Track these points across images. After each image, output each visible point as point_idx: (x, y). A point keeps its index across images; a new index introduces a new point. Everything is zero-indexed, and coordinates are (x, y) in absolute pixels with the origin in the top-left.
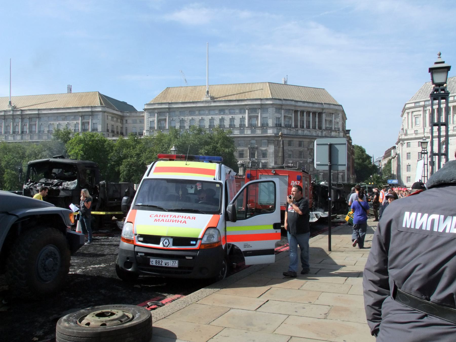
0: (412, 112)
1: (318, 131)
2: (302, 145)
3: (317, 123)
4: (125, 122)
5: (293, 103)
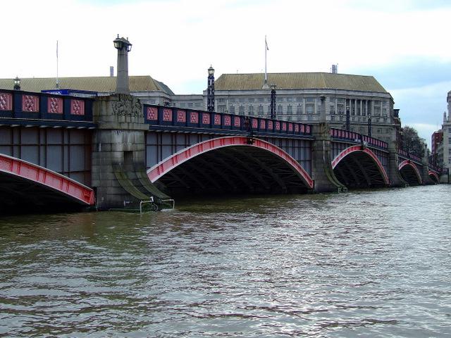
5: (345, 93)
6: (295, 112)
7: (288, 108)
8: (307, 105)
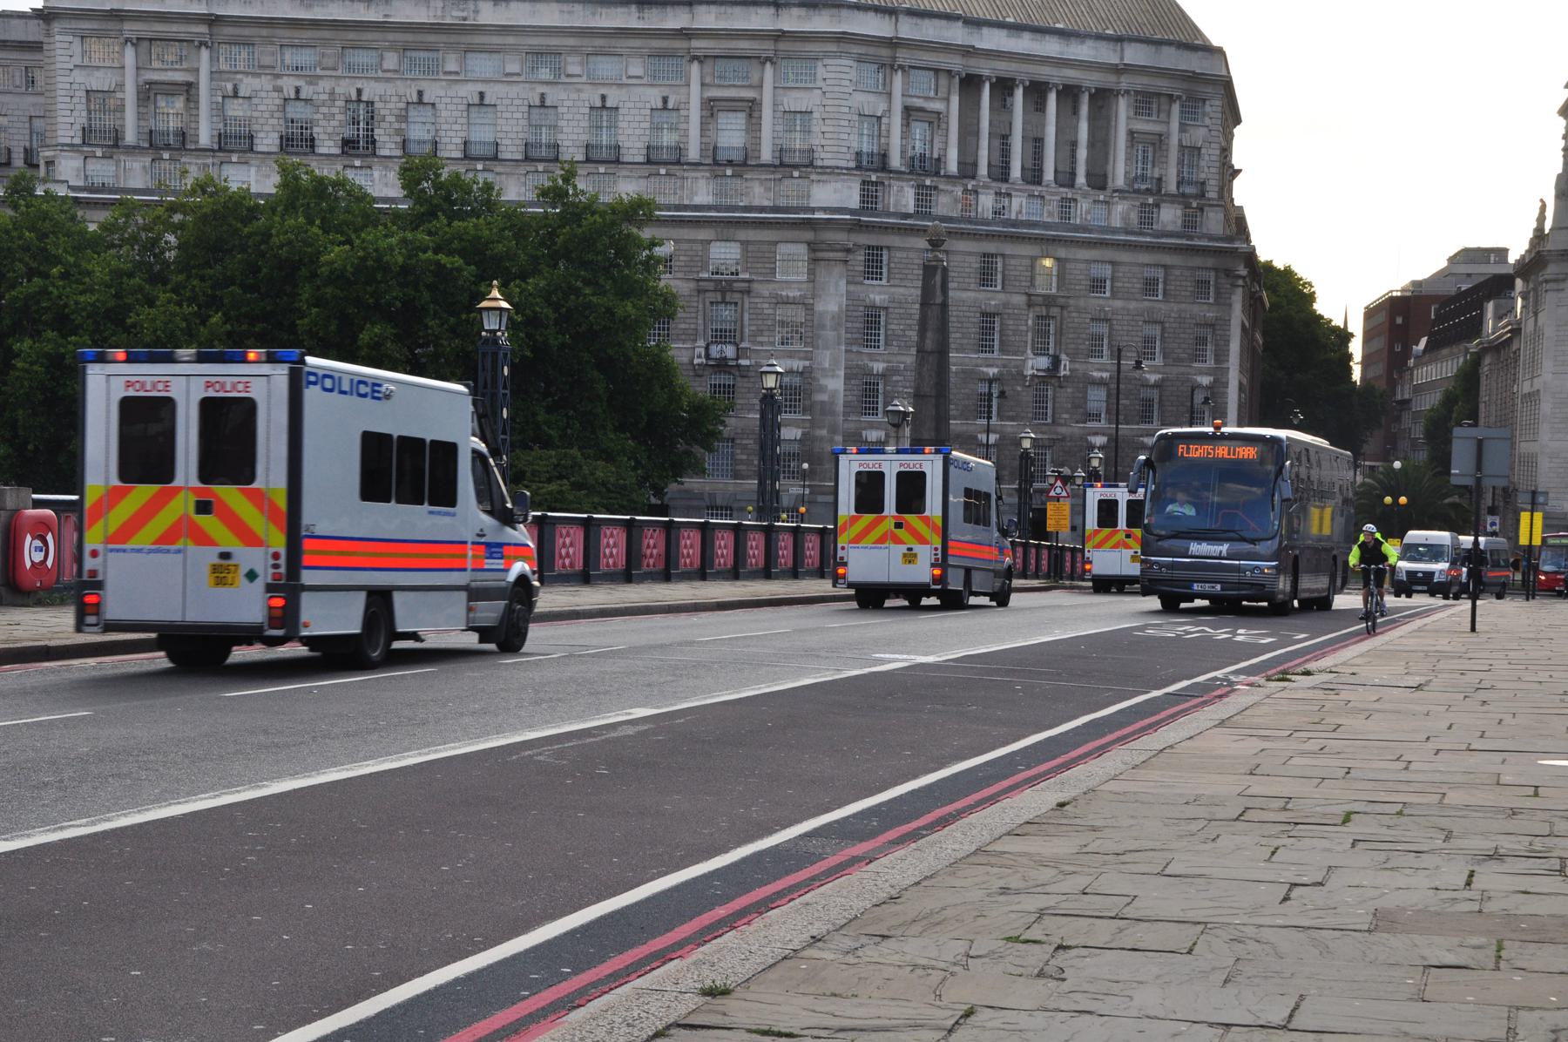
1: (1085, 196)
2: (999, 277)
3: (1082, 154)
5: (957, 34)
6: (634, 149)
8: (712, 108)
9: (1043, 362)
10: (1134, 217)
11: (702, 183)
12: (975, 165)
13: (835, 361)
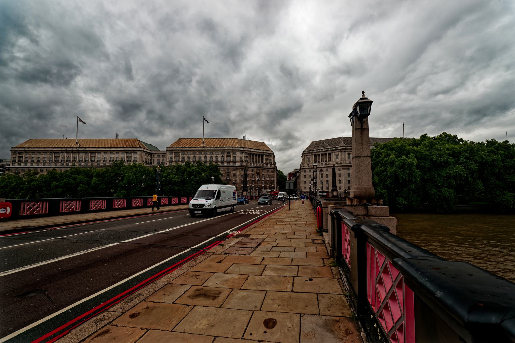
0: (306, 155)
3: (261, 160)
4: (153, 156)
5: (249, 150)
7: (216, 158)
8: (227, 156)
9: (258, 179)
10: (266, 166)
11: (226, 163)
12: (251, 161)
13: (238, 179)
